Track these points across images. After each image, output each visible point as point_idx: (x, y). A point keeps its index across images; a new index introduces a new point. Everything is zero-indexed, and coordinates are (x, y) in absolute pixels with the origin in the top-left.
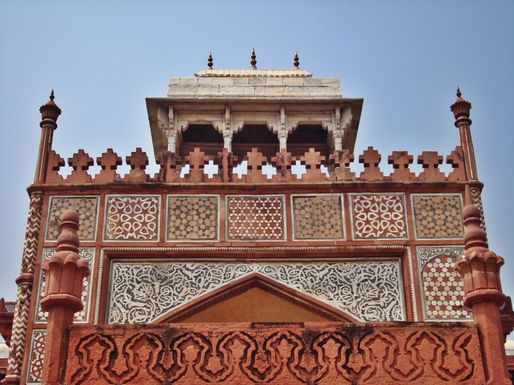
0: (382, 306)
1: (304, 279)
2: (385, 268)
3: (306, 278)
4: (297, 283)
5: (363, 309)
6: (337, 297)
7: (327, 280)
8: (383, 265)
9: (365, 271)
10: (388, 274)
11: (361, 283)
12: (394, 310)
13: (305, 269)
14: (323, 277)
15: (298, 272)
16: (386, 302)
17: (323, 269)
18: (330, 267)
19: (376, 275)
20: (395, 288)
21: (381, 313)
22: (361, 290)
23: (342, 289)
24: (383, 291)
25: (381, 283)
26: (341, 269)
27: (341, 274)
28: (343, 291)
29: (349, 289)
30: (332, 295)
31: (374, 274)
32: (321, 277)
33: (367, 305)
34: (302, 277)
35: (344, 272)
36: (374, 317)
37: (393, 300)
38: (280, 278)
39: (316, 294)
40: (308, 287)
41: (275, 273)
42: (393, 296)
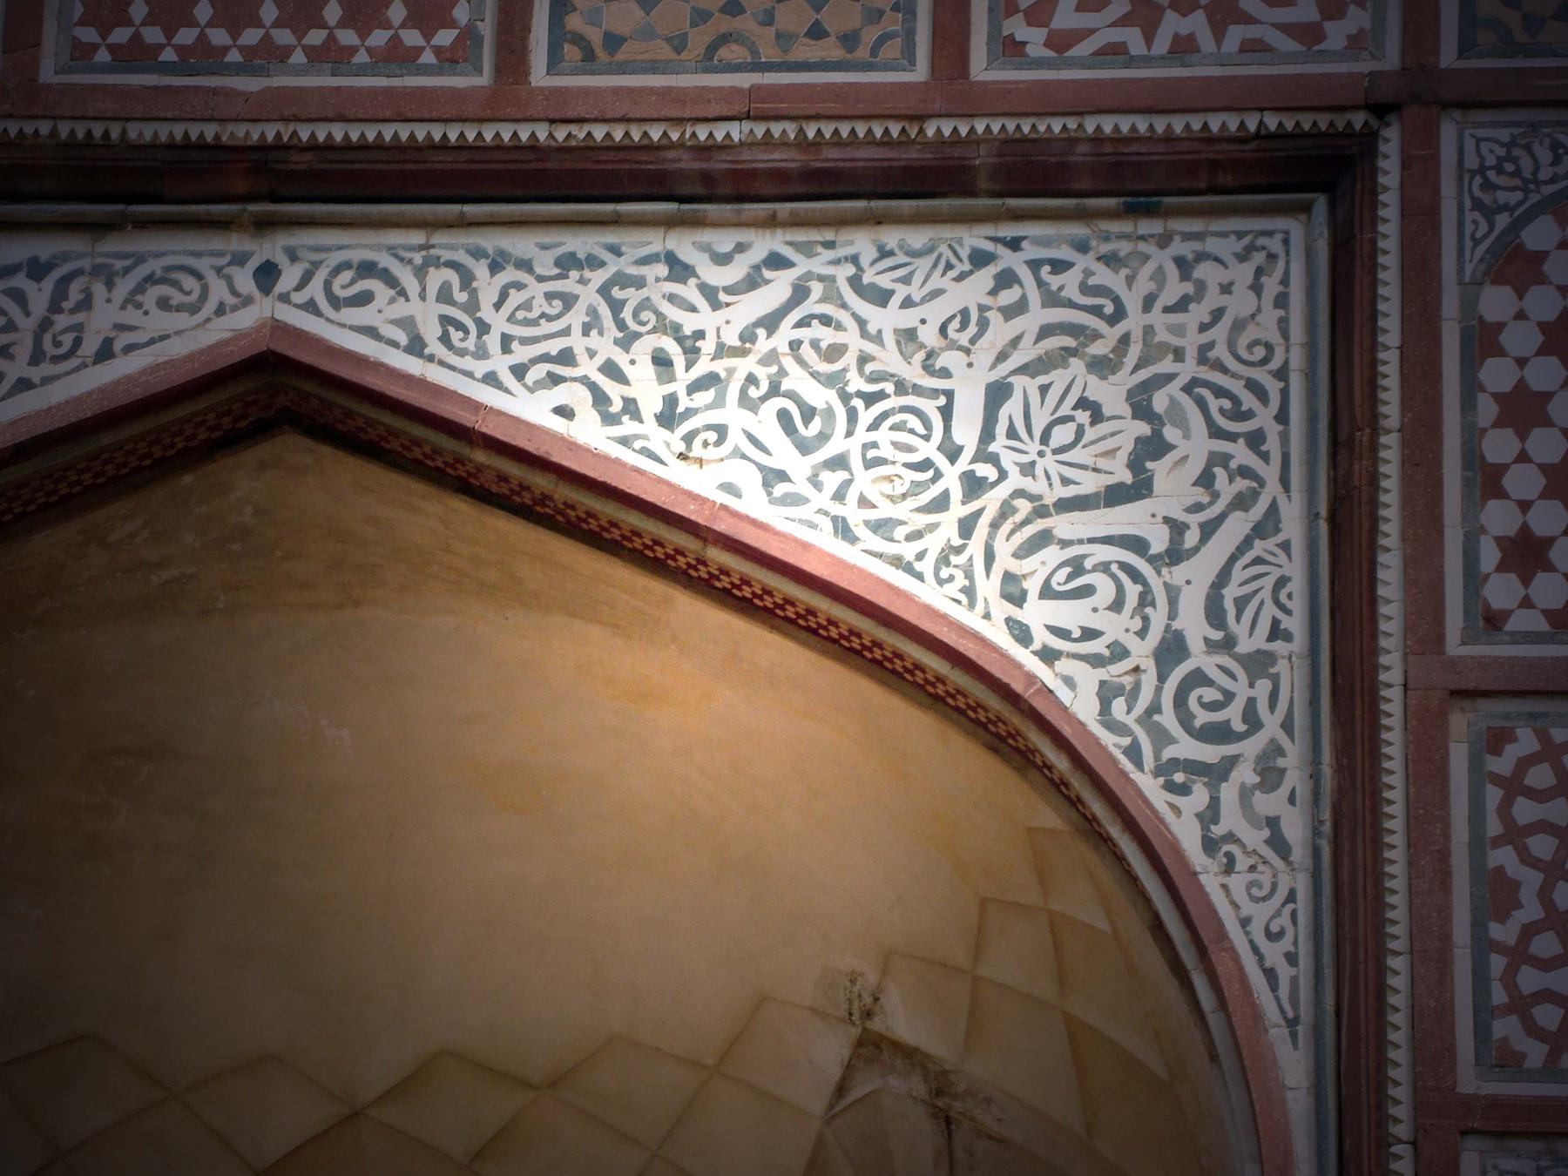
0: (1159, 545)
1: (606, 347)
2: (1200, 271)
3: (626, 342)
4: (555, 380)
5: (1017, 567)
6: (832, 480)
7: (771, 358)
8: (1186, 249)
9: (1052, 299)
10: (1217, 314)
11: (1019, 382)
12: (1238, 574)
13: (621, 280)
14: (748, 336)
15: (569, 301)
16: (1194, 520)
17: (752, 282)
18: (803, 265)
19: (1133, 323)
20: (1264, 418)
21: (1146, 599)
22: (1012, 433)
23: (874, 426)
24: (1171, 433)
25: (1170, 377)
26: (885, 281)
27: (877, 317)
28: (884, 435)
29: (927, 424)
30: (798, 466)
31: (1119, 315)
32: (732, 339)
33: (1043, 539)
34: (594, 340)
35: (907, 303)
36: (1094, 622)
37: (1242, 502)
38: (435, 347)
39: (682, 456)
40: (631, 408)
41: (401, 309)
42: (1244, 472)
